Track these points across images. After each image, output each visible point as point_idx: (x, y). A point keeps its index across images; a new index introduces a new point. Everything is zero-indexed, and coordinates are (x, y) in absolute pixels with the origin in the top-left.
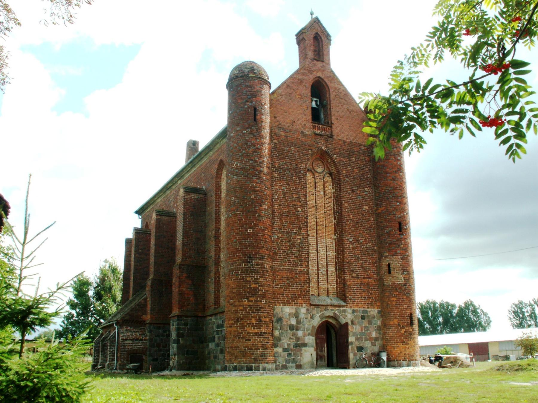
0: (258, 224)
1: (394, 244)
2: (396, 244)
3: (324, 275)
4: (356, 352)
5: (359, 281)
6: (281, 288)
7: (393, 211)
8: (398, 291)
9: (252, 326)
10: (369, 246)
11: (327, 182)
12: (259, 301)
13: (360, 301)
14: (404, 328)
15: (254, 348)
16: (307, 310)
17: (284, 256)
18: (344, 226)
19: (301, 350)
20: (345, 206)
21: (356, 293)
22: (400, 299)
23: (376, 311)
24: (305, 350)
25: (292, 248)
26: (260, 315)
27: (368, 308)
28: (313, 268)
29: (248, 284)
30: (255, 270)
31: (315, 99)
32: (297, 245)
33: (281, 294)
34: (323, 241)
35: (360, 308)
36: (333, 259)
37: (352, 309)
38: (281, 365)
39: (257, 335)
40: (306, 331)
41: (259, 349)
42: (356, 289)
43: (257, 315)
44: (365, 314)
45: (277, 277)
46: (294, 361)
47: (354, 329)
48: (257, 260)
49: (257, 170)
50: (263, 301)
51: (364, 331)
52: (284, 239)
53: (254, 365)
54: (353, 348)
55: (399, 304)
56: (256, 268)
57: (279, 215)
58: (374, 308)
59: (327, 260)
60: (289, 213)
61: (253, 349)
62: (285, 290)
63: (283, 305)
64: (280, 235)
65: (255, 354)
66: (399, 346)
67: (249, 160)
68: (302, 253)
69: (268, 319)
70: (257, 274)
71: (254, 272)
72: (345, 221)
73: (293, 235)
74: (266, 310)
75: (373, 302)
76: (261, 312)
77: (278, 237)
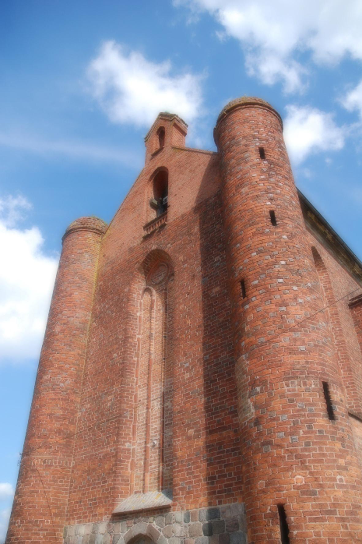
27: (220, 503)
58: (235, 500)
75: (231, 485)
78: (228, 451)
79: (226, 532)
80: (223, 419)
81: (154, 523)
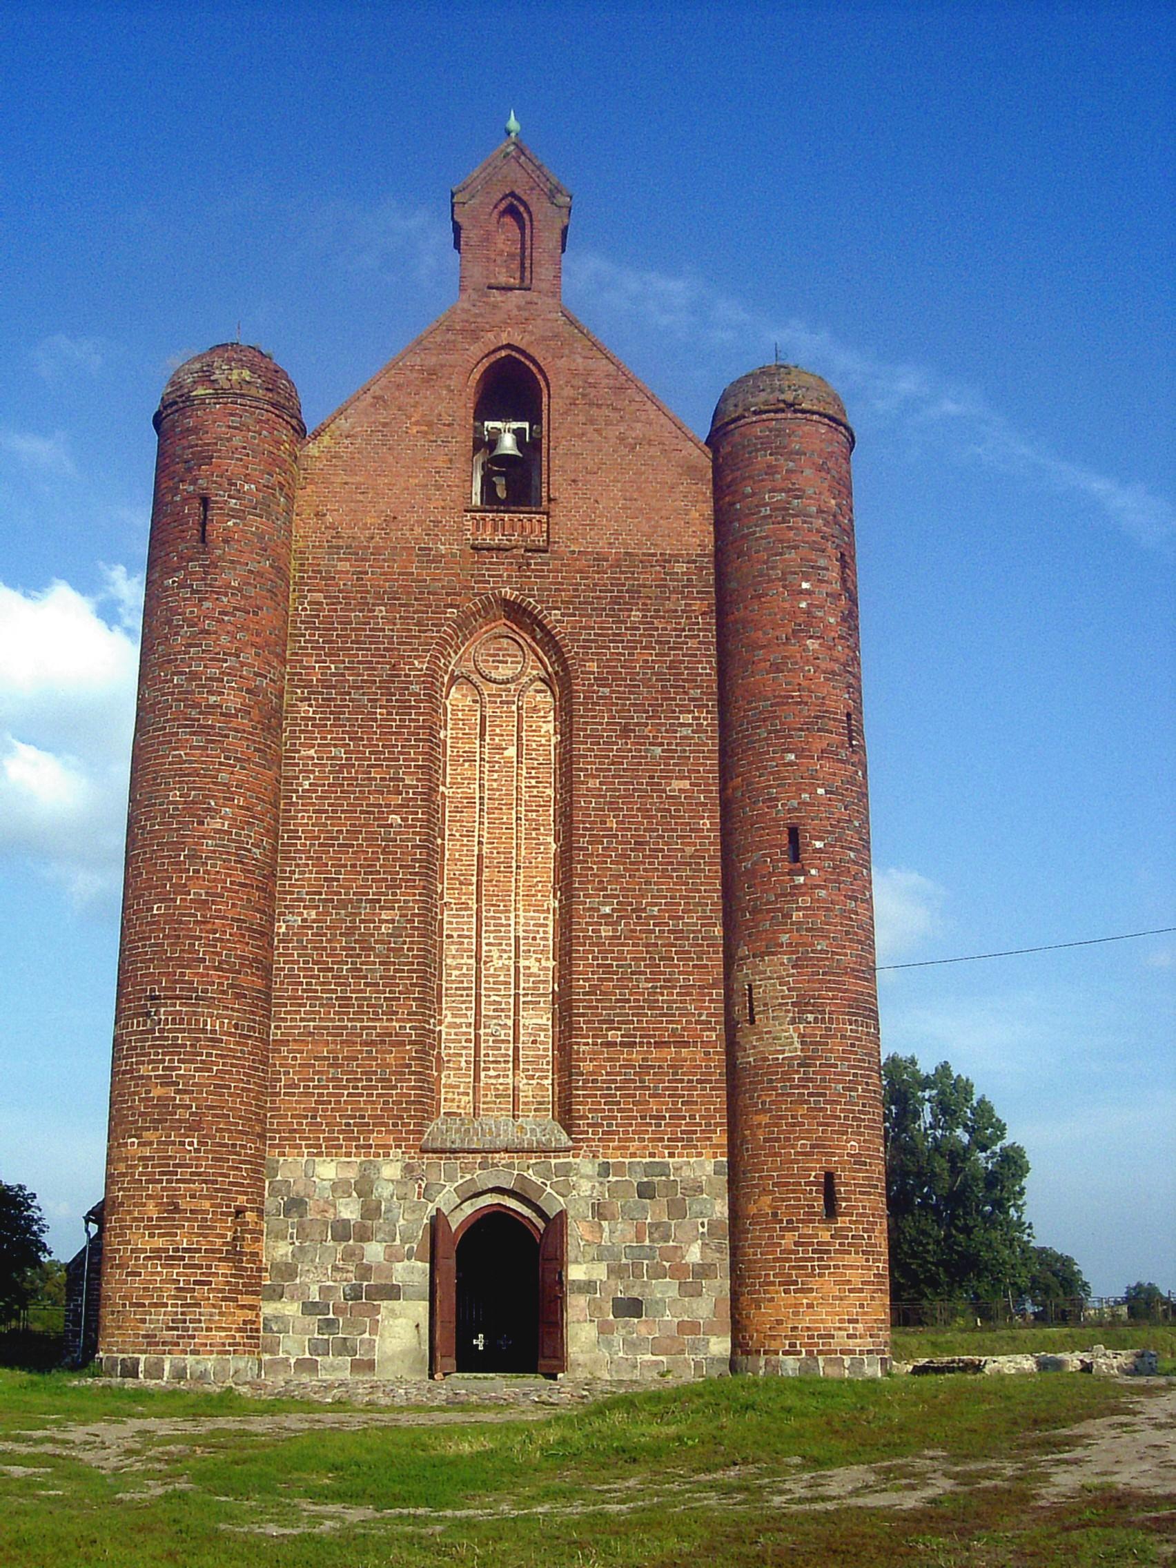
0: (185, 885)
1: (769, 911)
2: (773, 911)
3: (503, 1041)
4: (611, 1317)
5: (636, 1055)
6: (306, 1094)
7: (770, 787)
8: (775, 1089)
9: (146, 1228)
10: (687, 924)
11: (535, 709)
12: (173, 1143)
13: (634, 1132)
14: (795, 1229)
15: (147, 1302)
16: (408, 1168)
17: (323, 983)
18: (579, 862)
19: (377, 1309)
20: (588, 789)
21: (618, 1103)
22: (781, 1118)
23: (710, 1168)
24: (392, 1311)
25: (359, 956)
26: (175, 1189)
27: (671, 1155)
28: (458, 1021)
29: (143, 1085)
30: (167, 1039)
31: (515, 425)
32: (376, 942)
33: (306, 1117)
34: (504, 922)
35: (633, 1155)
36: (545, 982)
37: (601, 1160)
38: (292, 1361)
39: (160, 1258)
40: (398, 1242)
41: (166, 1305)
42: (617, 1089)
43: (163, 1189)
44: (656, 1179)
45: (295, 1058)
46: (344, 1347)
47: (606, 1234)
48: (174, 1005)
49: (196, 705)
50: (191, 1144)
51: (647, 1243)
52: (328, 928)
53: (143, 1357)
54: (595, 1306)
55: (778, 1140)
56: (170, 1031)
57: (312, 845)
58: (700, 1155)
59: (517, 987)
60: (354, 834)
61: (143, 1305)
62: (323, 1103)
63: (309, 1154)
64: (314, 912)
65: (151, 1322)
66: (772, 1300)
67: (174, 674)
68: (396, 971)
69: (206, 1205)
70: (172, 1053)
71: (163, 1046)
72: (583, 842)
73: (365, 910)
74: (200, 1174)
76: (178, 1181)
77: (304, 920)
78: (690, 1081)
79: (679, 1195)
80: (683, 1029)
81: (530, 1172)
